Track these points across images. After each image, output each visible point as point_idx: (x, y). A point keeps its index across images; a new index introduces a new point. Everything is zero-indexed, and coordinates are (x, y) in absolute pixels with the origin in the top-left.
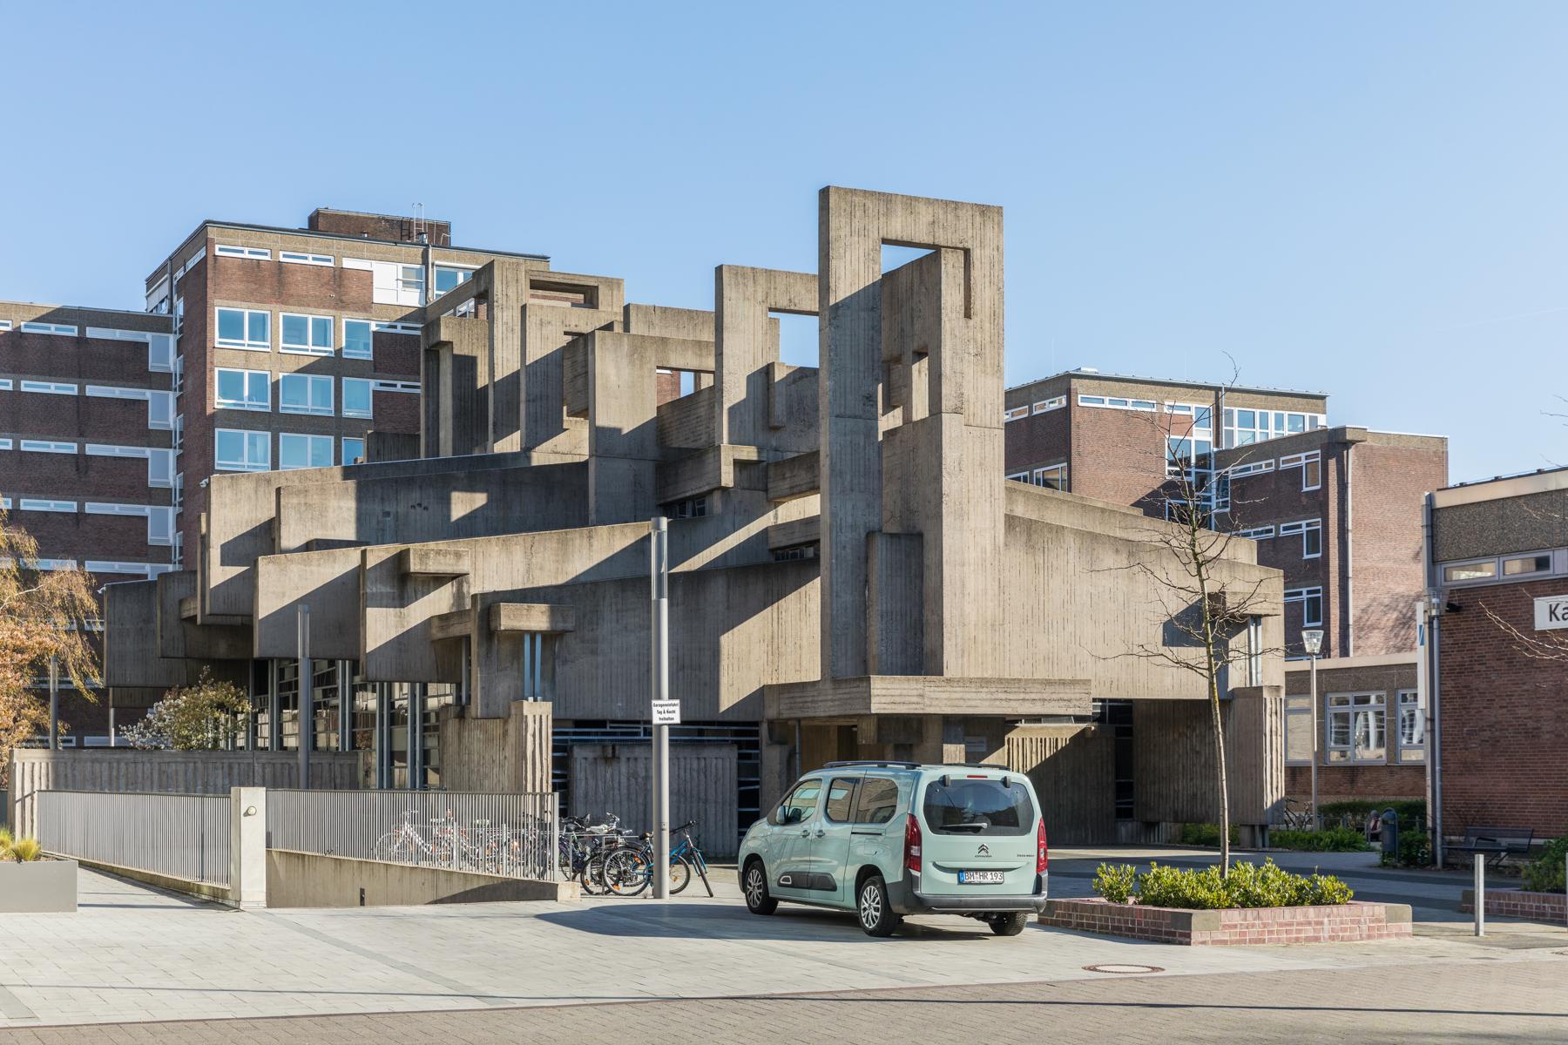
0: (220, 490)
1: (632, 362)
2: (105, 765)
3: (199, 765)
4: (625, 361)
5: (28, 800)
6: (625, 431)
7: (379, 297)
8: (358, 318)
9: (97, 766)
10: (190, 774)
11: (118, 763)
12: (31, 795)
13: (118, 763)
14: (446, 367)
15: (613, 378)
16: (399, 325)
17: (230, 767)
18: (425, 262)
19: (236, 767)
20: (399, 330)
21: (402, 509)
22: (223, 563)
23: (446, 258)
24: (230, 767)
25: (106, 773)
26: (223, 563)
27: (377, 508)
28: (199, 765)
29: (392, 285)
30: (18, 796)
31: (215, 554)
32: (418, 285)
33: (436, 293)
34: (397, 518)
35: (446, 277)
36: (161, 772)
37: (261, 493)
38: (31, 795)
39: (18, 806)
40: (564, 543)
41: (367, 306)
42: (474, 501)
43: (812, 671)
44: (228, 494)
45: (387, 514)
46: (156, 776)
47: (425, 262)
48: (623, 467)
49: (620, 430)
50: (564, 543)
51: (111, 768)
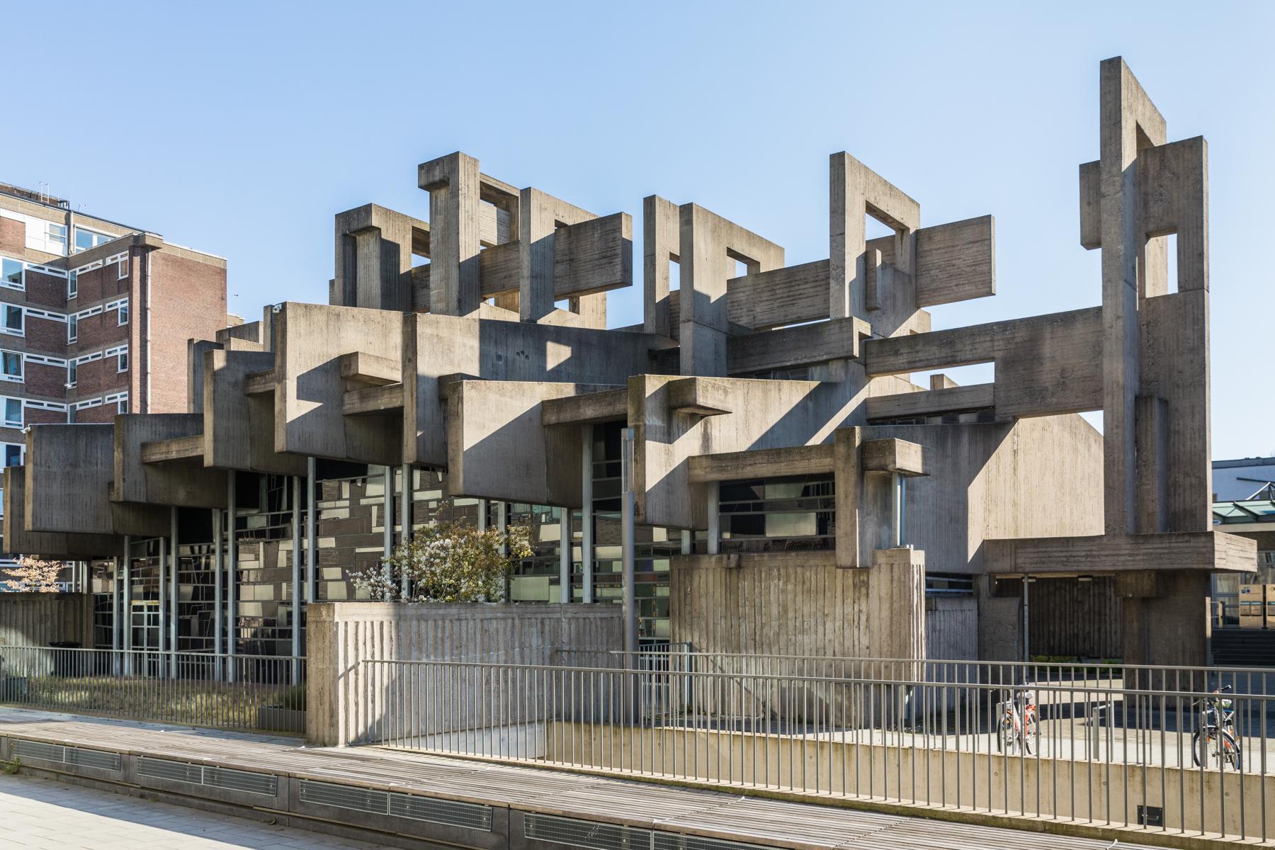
0: (296, 317)
1: (713, 239)
2: (431, 623)
3: (517, 621)
4: (709, 240)
5: (352, 674)
6: (712, 301)
7: (29, 244)
8: (14, 258)
9: (423, 624)
10: (509, 633)
11: (443, 620)
12: (355, 667)
13: (443, 620)
14: (368, 252)
15: (703, 251)
16: (47, 268)
17: (543, 623)
18: (68, 223)
19: (547, 622)
20: (46, 272)
21: (510, 354)
22: (299, 397)
23: (84, 223)
24: (543, 623)
25: (431, 635)
26: (299, 397)
27: (492, 350)
28: (517, 621)
29: (42, 240)
30: (341, 670)
31: (292, 386)
32: (62, 239)
33: (76, 249)
34: (506, 361)
35: (84, 238)
36: (485, 631)
37: (331, 327)
38: (355, 667)
39: (341, 682)
40: (765, 392)
41: (21, 249)
42: (559, 355)
43: (1096, 526)
44: (303, 323)
45: (499, 358)
46: (479, 637)
47: (68, 223)
48: (708, 334)
49: (709, 298)
50: (765, 392)
51: (436, 627)
